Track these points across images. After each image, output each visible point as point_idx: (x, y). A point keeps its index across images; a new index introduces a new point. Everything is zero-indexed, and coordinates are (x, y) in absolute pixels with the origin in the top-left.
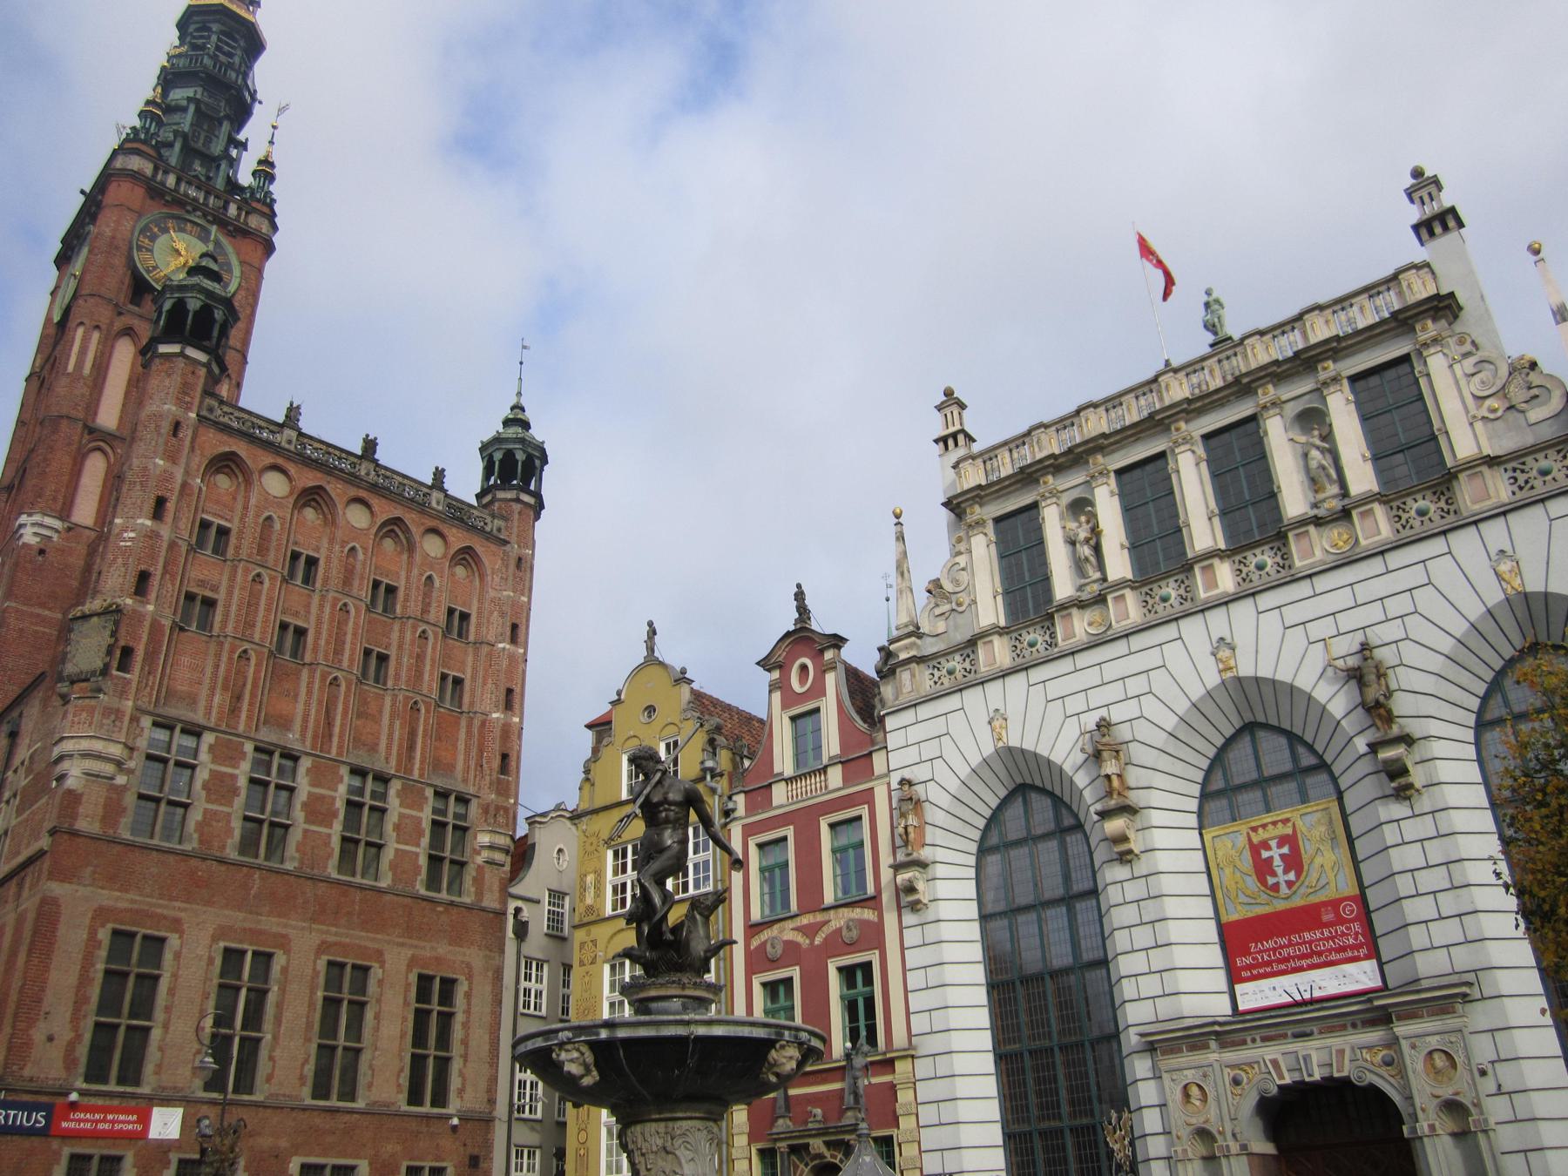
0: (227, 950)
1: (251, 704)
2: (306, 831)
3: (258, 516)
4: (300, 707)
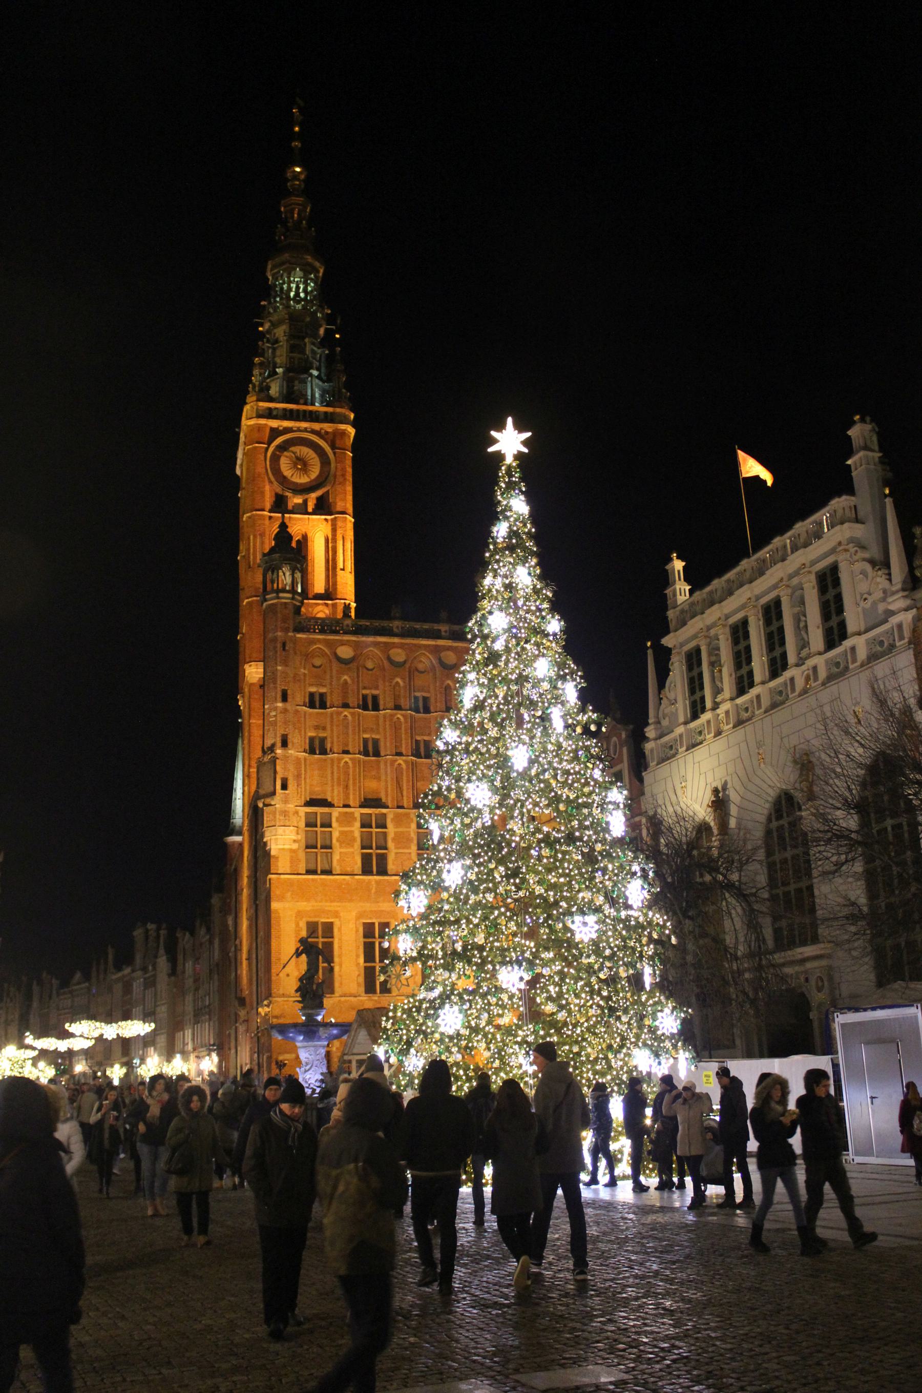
0: (364, 924)
1: (354, 790)
2: (396, 853)
3: (339, 679)
4: (383, 784)
